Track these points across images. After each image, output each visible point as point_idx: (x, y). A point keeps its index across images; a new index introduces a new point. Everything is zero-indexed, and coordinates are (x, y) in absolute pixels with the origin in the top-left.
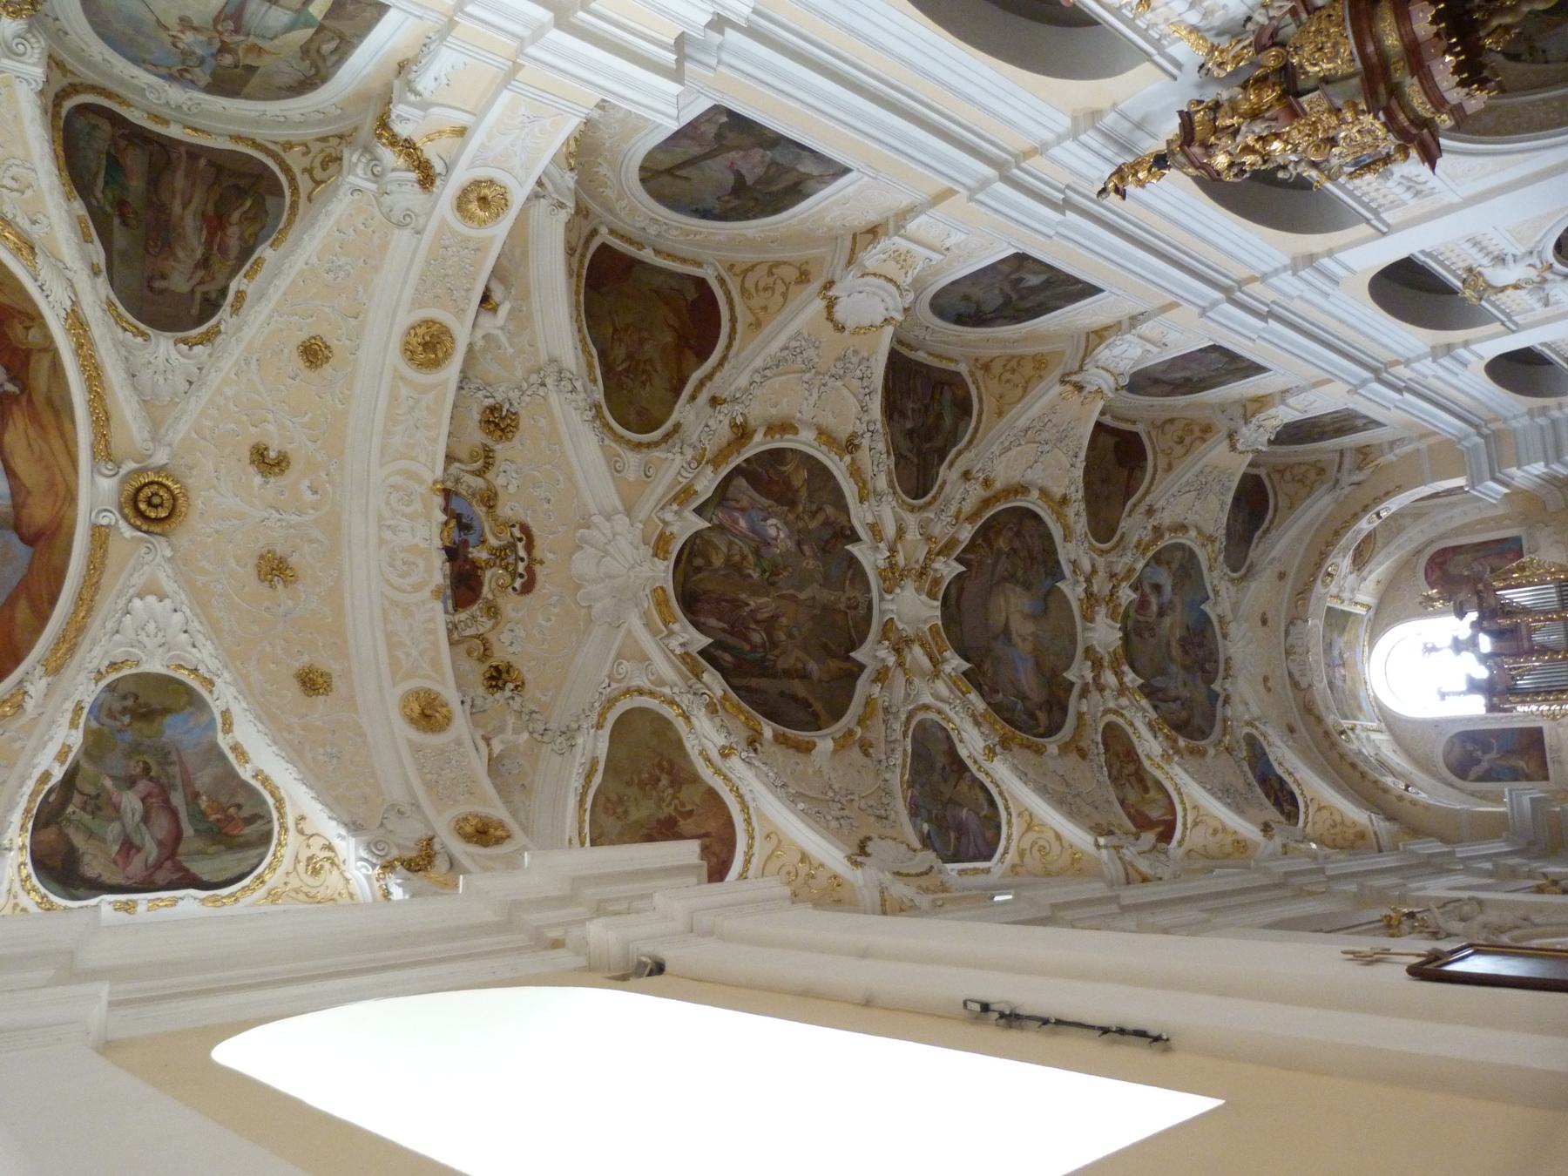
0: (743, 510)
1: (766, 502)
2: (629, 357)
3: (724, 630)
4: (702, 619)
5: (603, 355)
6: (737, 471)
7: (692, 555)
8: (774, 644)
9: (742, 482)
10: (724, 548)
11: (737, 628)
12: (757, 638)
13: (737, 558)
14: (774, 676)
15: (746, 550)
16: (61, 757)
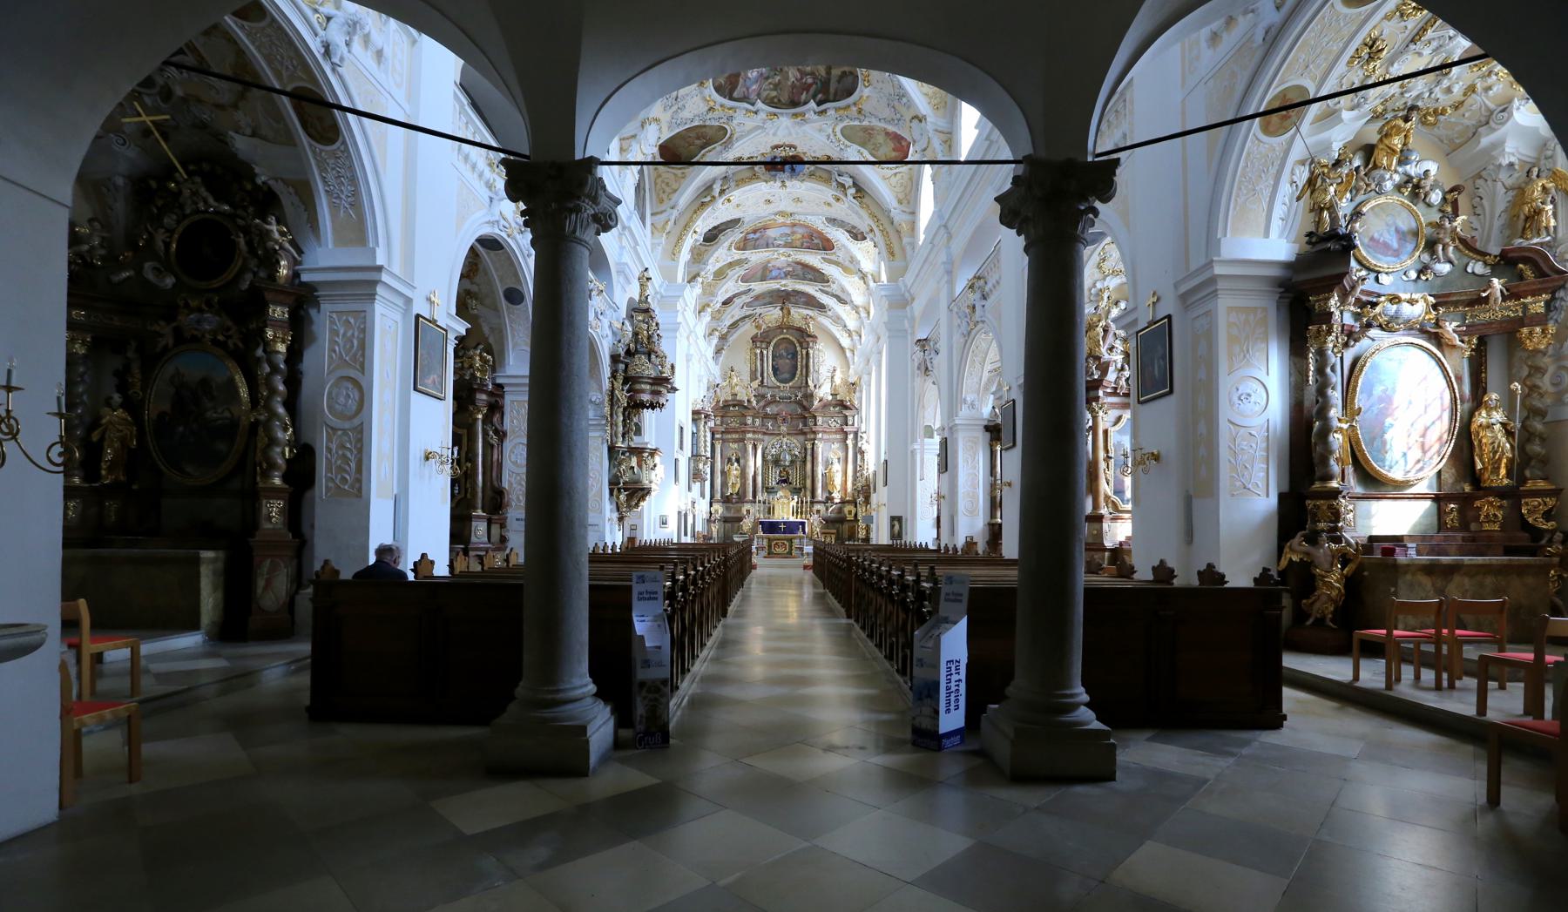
0: (748, 89)
1: (741, 80)
2: (698, 138)
3: (807, 93)
4: (802, 101)
5: (703, 147)
6: (731, 99)
7: (774, 103)
8: (812, 74)
9: (735, 95)
10: (768, 92)
11: (807, 88)
12: (810, 81)
13: (771, 86)
14: (829, 80)
15: (767, 83)
16: (843, 233)
